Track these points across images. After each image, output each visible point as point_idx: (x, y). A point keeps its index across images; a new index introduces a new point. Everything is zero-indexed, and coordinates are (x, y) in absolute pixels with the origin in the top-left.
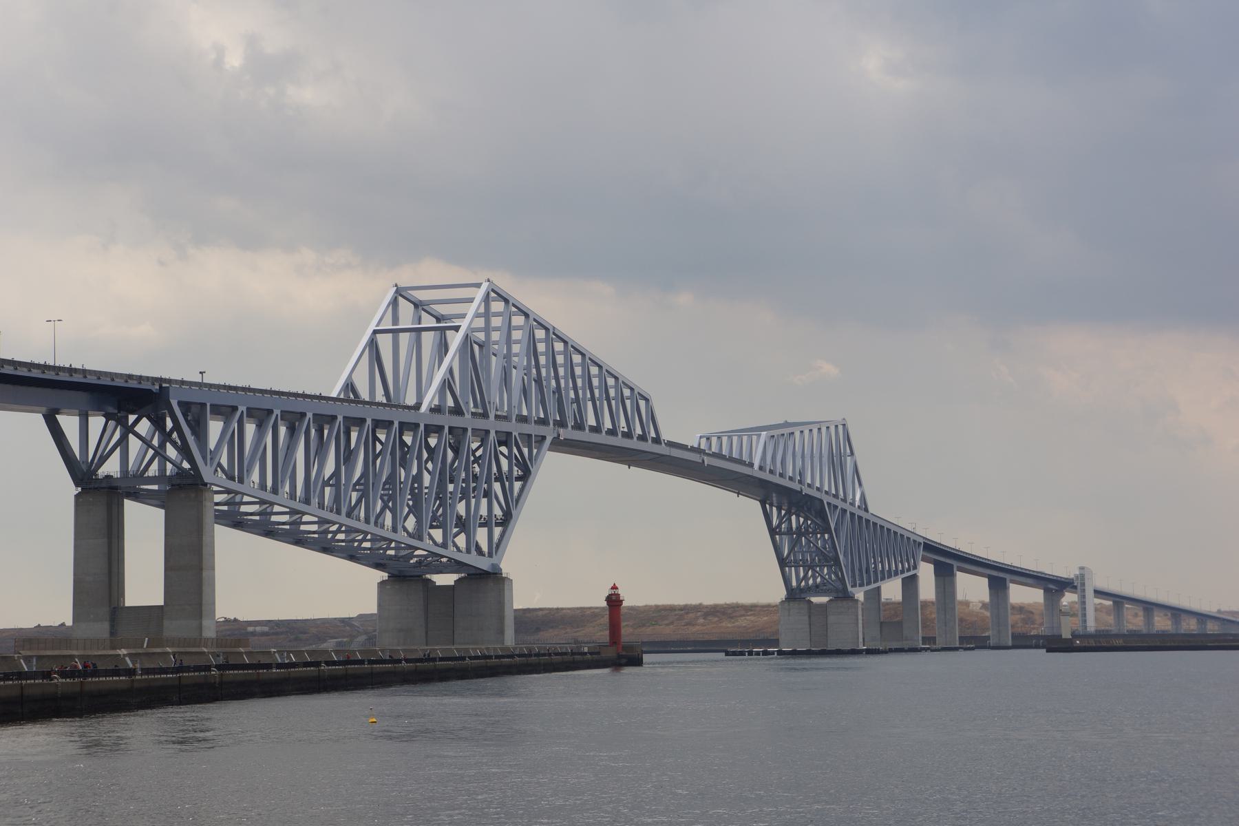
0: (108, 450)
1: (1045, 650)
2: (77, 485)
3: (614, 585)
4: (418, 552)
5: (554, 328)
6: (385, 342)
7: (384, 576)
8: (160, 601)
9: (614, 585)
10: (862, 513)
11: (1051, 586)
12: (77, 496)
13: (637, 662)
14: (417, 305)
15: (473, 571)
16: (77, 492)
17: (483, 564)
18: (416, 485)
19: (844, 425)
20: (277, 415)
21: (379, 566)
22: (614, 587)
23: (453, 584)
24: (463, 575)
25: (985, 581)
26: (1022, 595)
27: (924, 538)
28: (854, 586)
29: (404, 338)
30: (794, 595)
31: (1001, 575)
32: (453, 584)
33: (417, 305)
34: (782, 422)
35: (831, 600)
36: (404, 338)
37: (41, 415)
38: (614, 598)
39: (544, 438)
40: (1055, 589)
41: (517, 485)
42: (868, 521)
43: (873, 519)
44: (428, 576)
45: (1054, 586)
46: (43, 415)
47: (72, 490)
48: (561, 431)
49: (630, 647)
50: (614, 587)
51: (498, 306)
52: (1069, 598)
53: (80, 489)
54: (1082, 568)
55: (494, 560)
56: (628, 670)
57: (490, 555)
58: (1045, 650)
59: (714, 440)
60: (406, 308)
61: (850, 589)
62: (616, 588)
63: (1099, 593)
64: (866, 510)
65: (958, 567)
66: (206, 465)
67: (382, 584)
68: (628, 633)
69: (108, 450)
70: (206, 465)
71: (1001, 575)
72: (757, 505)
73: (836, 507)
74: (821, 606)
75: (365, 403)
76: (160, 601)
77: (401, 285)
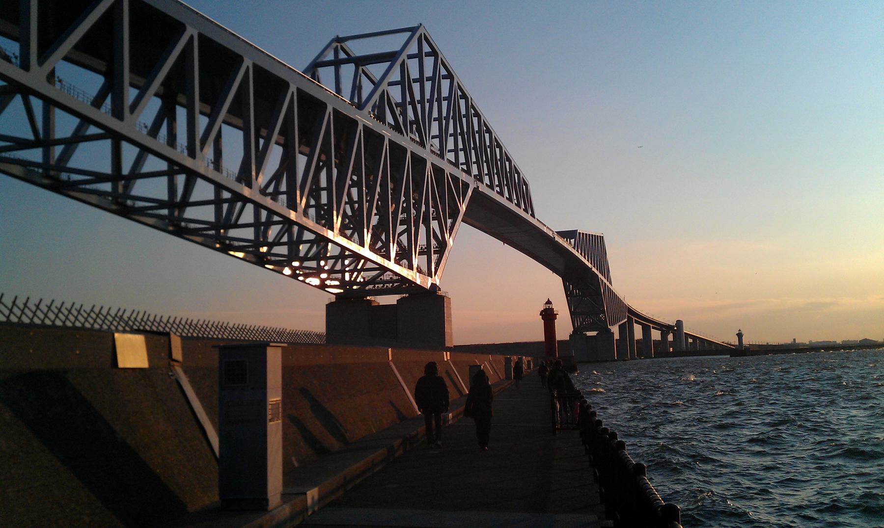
0: (88, 187)
3: (549, 300)
9: (549, 300)
10: (610, 286)
18: (356, 205)
22: (549, 302)
26: (656, 335)
28: (610, 325)
38: (549, 312)
45: (665, 329)
48: (480, 184)
50: (549, 302)
54: (677, 321)
64: (610, 283)
69: (88, 187)
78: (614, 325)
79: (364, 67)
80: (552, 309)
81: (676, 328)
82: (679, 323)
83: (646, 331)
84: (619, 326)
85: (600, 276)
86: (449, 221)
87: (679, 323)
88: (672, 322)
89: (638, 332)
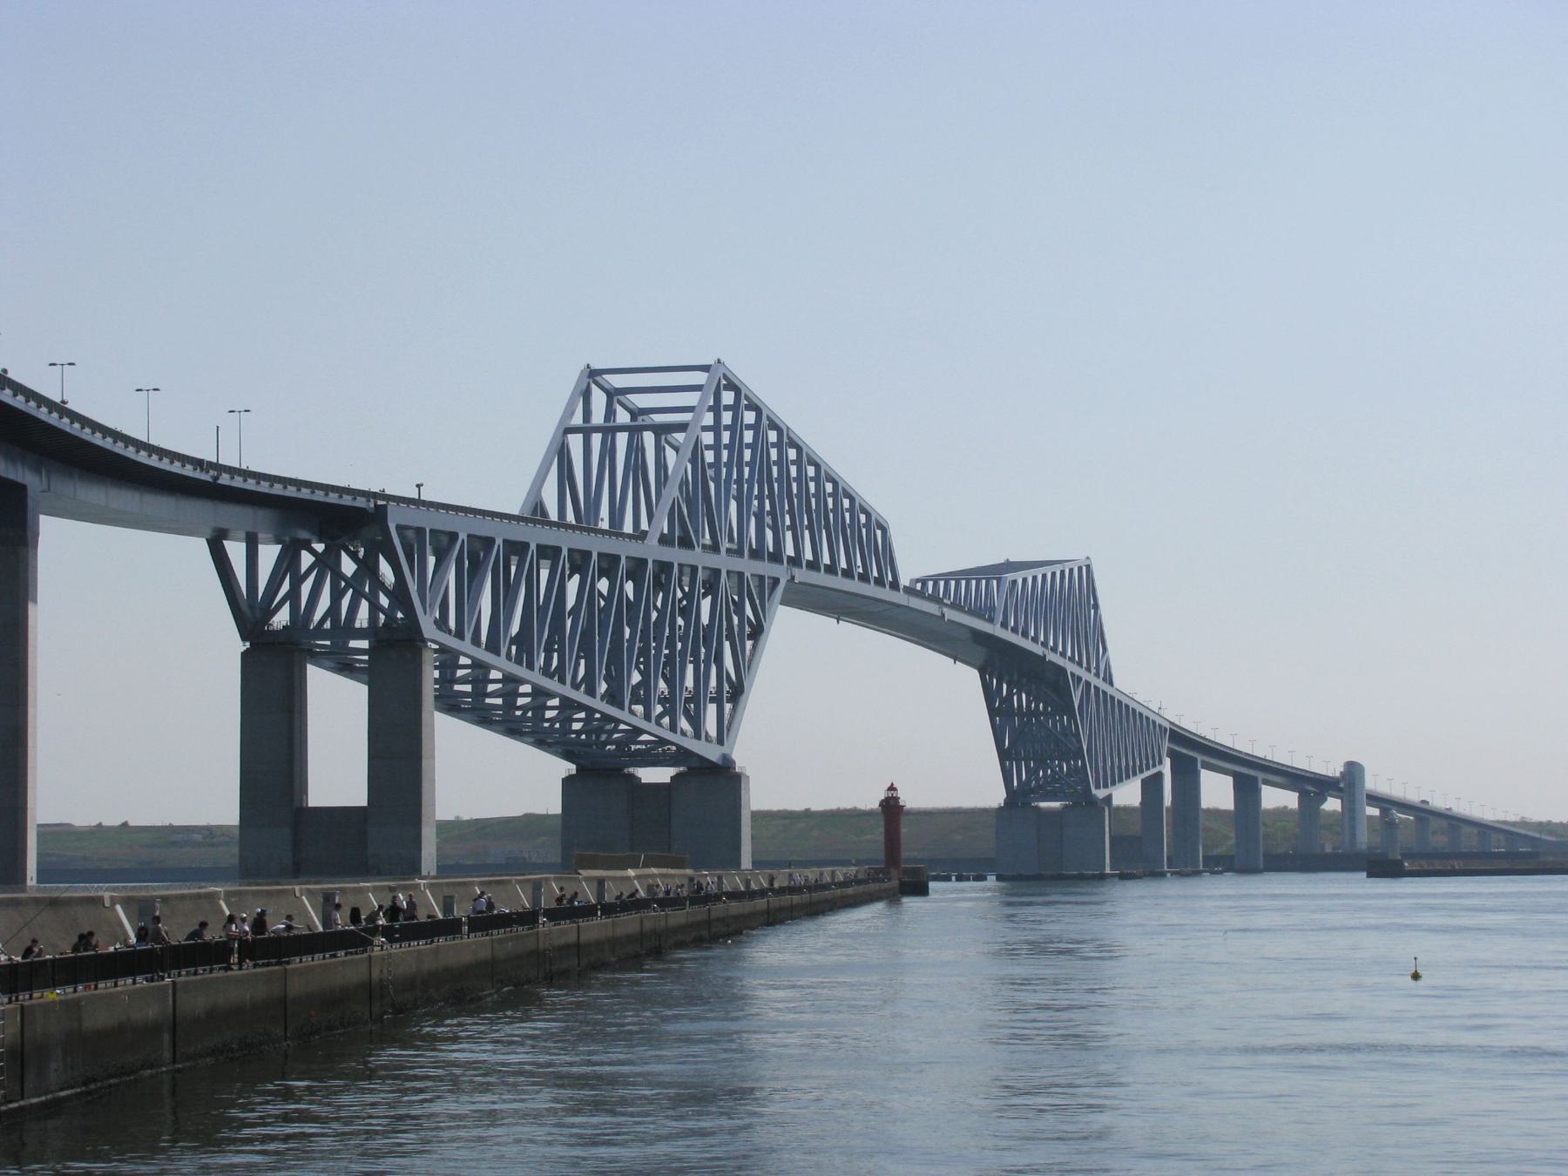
1: (1365, 874)
2: (244, 638)
3: (892, 784)
4: (645, 737)
5: (788, 428)
6: (575, 442)
7: (571, 768)
8: (362, 801)
9: (892, 784)
10: (1104, 686)
11: (1310, 788)
12: (245, 655)
13: (921, 890)
14: (612, 394)
15: (695, 763)
16: (245, 648)
17: (712, 753)
19: (1088, 567)
20: (463, 541)
21: (568, 756)
22: (892, 788)
23: (668, 781)
24: (681, 769)
25: (1228, 781)
26: (1275, 798)
27: (1171, 723)
28: (1098, 787)
29: (596, 439)
30: (1016, 798)
31: (1252, 772)
32: (668, 781)
33: (612, 394)
34: (1003, 562)
35: (1066, 807)
36: (596, 439)
37: (204, 540)
38: (892, 802)
39: (776, 581)
40: (1314, 792)
41: (749, 644)
42: (1112, 698)
43: (1118, 696)
44: (631, 770)
45: (1310, 785)
46: (207, 540)
47: (234, 646)
48: (796, 571)
49: (916, 872)
50: (892, 788)
51: (728, 398)
52: (1332, 804)
53: (248, 644)
55: (724, 750)
56: (911, 903)
57: (720, 741)
58: (1365, 874)
59: (931, 584)
60: (599, 399)
61: (1094, 791)
62: (895, 789)
63: (1374, 799)
64: (1111, 683)
65: (1203, 762)
66: (425, 614)
67: (567, 782)
68: (910, 851)
70: (425, 614)
71: (1252, 772)
72: (974, 675)
73: (1079, 679)
74: (1051, 813)
75: (551, 524)
76: (362, 801)
77: (596, 366)
78: (1121, 780)
79: (619, 397)
80: (897, 799)
81: (1342, 785)
82: (1353, 771)
83: (1246, 789)
84: (1142, 780)
85: (1071, 668)
86: (749, 644)
87: (1353, 771)
88: (1333, 769)
89: (1216, 791)
